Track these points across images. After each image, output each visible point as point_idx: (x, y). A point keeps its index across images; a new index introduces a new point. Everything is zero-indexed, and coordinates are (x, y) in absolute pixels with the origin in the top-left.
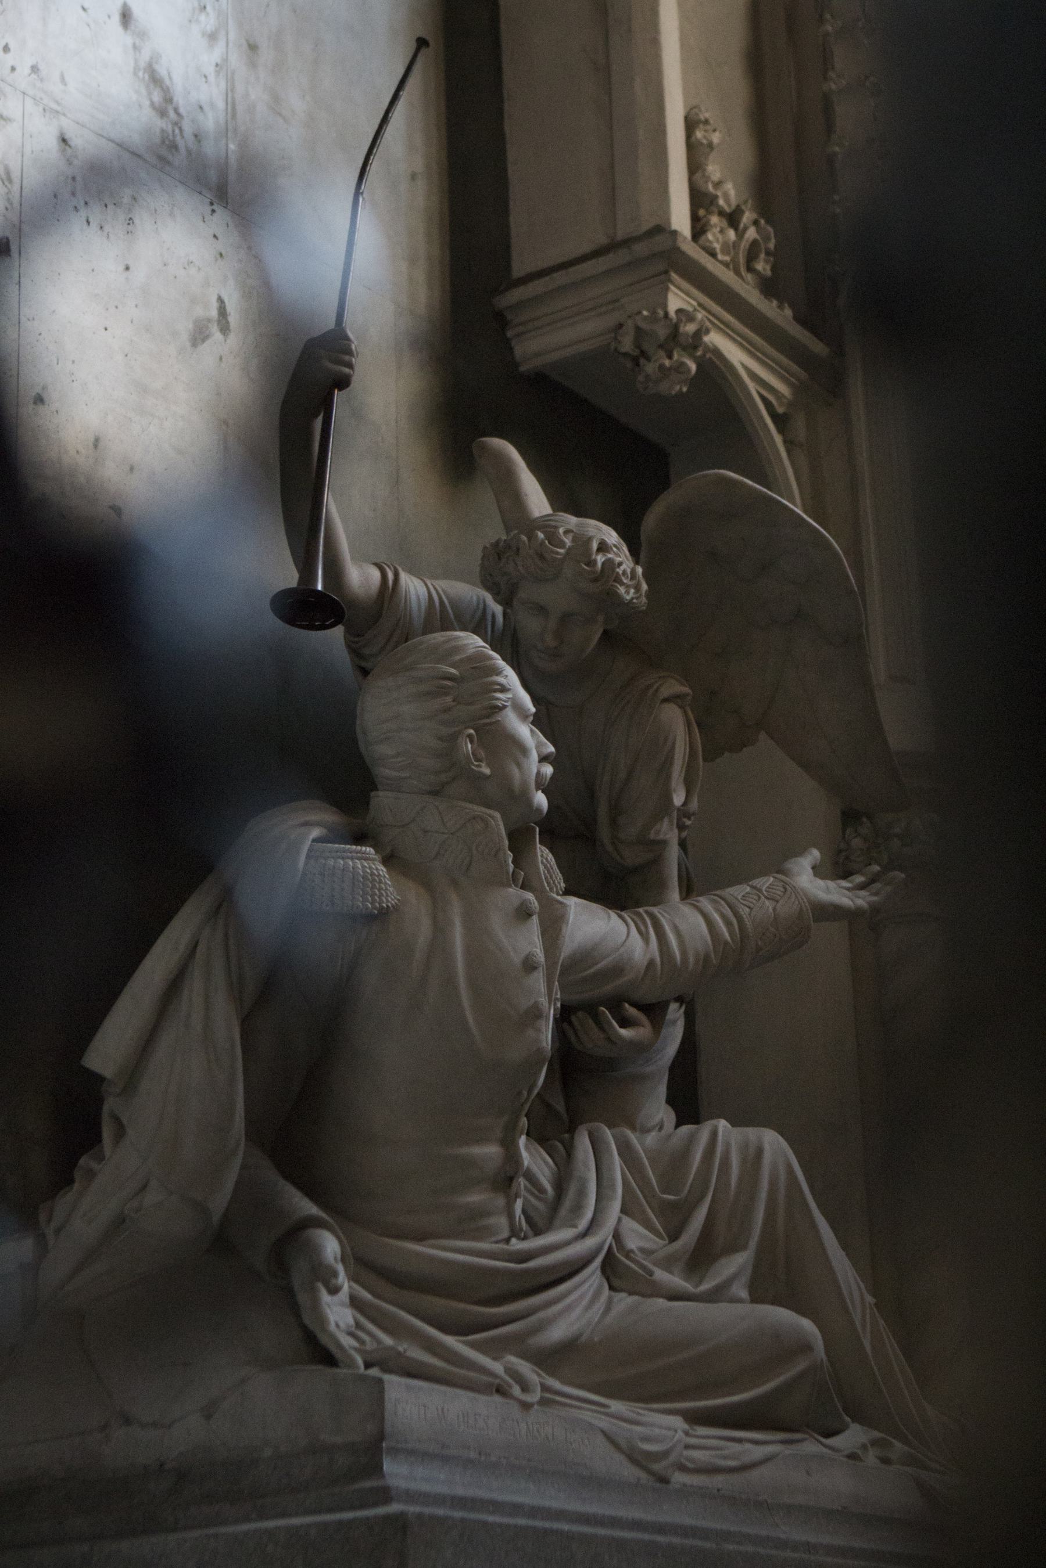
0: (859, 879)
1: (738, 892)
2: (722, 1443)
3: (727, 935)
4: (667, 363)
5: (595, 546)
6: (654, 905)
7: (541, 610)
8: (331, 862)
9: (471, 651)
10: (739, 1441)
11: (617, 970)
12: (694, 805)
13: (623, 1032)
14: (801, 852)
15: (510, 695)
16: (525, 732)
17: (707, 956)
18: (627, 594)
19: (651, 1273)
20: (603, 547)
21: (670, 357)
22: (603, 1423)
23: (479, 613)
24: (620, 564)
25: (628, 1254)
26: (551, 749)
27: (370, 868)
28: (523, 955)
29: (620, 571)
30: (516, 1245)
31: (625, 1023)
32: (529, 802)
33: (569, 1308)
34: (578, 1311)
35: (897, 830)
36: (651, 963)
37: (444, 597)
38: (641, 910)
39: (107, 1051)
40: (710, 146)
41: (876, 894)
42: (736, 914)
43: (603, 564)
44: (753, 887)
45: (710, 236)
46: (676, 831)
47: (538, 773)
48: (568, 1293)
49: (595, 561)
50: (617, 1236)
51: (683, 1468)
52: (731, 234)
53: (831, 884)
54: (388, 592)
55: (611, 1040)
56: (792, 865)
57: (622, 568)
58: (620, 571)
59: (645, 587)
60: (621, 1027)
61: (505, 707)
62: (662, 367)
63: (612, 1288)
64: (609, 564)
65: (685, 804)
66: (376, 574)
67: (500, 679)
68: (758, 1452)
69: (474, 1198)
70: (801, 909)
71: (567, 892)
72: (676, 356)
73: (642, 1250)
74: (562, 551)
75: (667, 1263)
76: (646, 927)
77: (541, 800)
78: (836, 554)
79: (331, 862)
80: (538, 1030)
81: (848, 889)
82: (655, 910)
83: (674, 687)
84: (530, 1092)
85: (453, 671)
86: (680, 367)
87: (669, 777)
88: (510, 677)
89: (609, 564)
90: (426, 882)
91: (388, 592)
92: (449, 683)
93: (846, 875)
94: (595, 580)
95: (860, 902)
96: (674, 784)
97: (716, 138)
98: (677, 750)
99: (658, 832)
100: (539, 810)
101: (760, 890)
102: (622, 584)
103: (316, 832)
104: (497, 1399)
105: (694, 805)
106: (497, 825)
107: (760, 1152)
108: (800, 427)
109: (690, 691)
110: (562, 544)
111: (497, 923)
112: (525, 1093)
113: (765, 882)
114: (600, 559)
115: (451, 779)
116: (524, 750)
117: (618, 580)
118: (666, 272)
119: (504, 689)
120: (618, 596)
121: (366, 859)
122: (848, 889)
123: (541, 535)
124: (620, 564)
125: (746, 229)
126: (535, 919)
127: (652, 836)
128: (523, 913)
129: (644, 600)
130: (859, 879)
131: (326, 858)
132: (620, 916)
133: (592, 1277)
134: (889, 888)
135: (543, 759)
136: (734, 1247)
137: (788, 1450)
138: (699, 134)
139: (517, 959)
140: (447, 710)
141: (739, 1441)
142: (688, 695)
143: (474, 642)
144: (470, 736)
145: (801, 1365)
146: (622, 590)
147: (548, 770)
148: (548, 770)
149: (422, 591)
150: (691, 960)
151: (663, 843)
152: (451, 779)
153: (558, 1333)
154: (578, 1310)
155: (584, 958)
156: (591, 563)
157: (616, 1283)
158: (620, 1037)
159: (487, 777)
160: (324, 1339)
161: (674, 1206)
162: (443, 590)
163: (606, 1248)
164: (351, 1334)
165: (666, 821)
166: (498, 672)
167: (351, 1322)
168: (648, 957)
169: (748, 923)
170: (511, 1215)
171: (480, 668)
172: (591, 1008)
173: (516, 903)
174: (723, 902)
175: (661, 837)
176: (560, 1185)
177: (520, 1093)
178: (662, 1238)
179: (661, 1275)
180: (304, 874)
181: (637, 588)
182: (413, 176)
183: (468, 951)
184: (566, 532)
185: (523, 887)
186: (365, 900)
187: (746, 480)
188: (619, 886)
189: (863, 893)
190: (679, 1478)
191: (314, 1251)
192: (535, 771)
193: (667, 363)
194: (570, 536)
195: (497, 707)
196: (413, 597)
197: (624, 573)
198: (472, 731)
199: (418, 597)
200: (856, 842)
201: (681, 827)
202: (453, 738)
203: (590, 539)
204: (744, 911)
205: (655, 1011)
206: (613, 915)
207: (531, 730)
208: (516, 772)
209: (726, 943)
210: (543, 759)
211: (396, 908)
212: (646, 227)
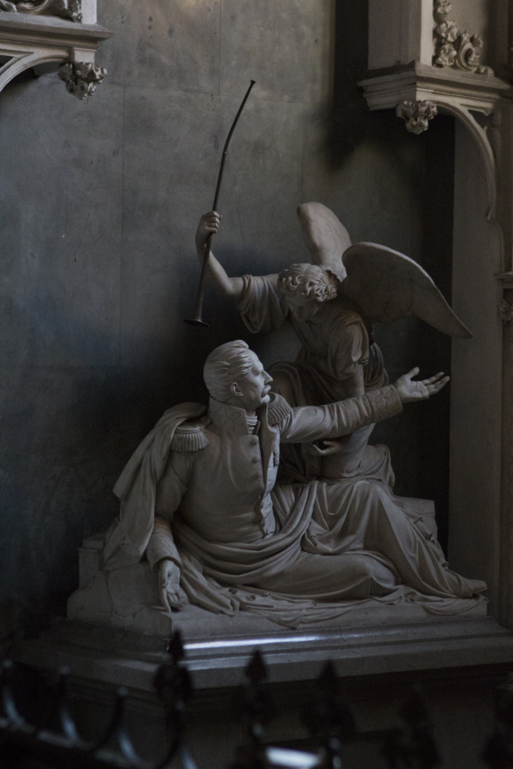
0: (434, 379)
2: (322, 611)
3: (366, 414)
4: (415, 123)
5: (308, 285)
8: (182, 435)
10: (334, 608)
13: (323, 452)
19: (315, 545)
20: (311, 284)
21: (416, 120)
22: (267, 614)
25: (311, 538)
26: (271, 379)
29: (318, 292)
32: (259, 402)
33: (281, 561)
34: (284, 562)
36: (334, 428)
37: (271, 286)
40: (445, 13)
41: (436, 388)
42: (371, 405)
43: (310, 292)
45: (440, 59)
47: (262, 392)
48: (279, 557)
50: (308, 531)
51: (303, 623)
52: (454, 53)
56: (399, 381)
62: (412, 125)
63: (302, 550)
65: (361, 357)
67: (246, 365)
68: (339, 611)
69: (245, 529)
72: (418, 119)
73: (317, 535)
74: (296, 287)
79: (182, 435)
85: (228, 364)
86: (421, 125)
89: (312, 291)
90: (220, 435)
96: (353, 353)
97: (448, 9)
104: (221, 615)
107: (368, 496)
108: (499, 119)
112: (260, 497)
114: (309, 289)
115: (229, 400)
116: (255, 386)
117: (317, 295)
118: (415, 83)
122: (426, 385)
125: (464, 45)
127: (346, 371)
128: (253, 444)
131: (180, 434)
133: (297, 546)
136: (353, 532)
137: (357, 607)
138: (439, 10)
139: (250, 460)
140: (226, 377)
141: (334, 608)
145: (362, 580)
147: (269, 388)
152: (229, 400)
153: (274, 571)
154: (279, 565)
156: (305, 292)
157: (305, 548)
161: (333, 517)
163: (302, 534)
165: (352, 366)
169: (375, 409)
170: (262, 531)
171: (238, 362)
174: (367, 400)
175: (350, 371)
176: (294, 508)
177: (257, 498)
178: (326, 528)
179: (321, 546)
180: (173, 439)
182: (316, 41)
184: (299, 278)
189: (432, 386)
190: (301, 626)
192: (261, 391)
193: (415, 123)
196: (256, 288)
198: (235, 383)
202: (228, 387)
204: (374, 404)
208: (253, 394)
209: (366, 417)
210: (266, 384)
211: (208, 446)
212: (410, 60)
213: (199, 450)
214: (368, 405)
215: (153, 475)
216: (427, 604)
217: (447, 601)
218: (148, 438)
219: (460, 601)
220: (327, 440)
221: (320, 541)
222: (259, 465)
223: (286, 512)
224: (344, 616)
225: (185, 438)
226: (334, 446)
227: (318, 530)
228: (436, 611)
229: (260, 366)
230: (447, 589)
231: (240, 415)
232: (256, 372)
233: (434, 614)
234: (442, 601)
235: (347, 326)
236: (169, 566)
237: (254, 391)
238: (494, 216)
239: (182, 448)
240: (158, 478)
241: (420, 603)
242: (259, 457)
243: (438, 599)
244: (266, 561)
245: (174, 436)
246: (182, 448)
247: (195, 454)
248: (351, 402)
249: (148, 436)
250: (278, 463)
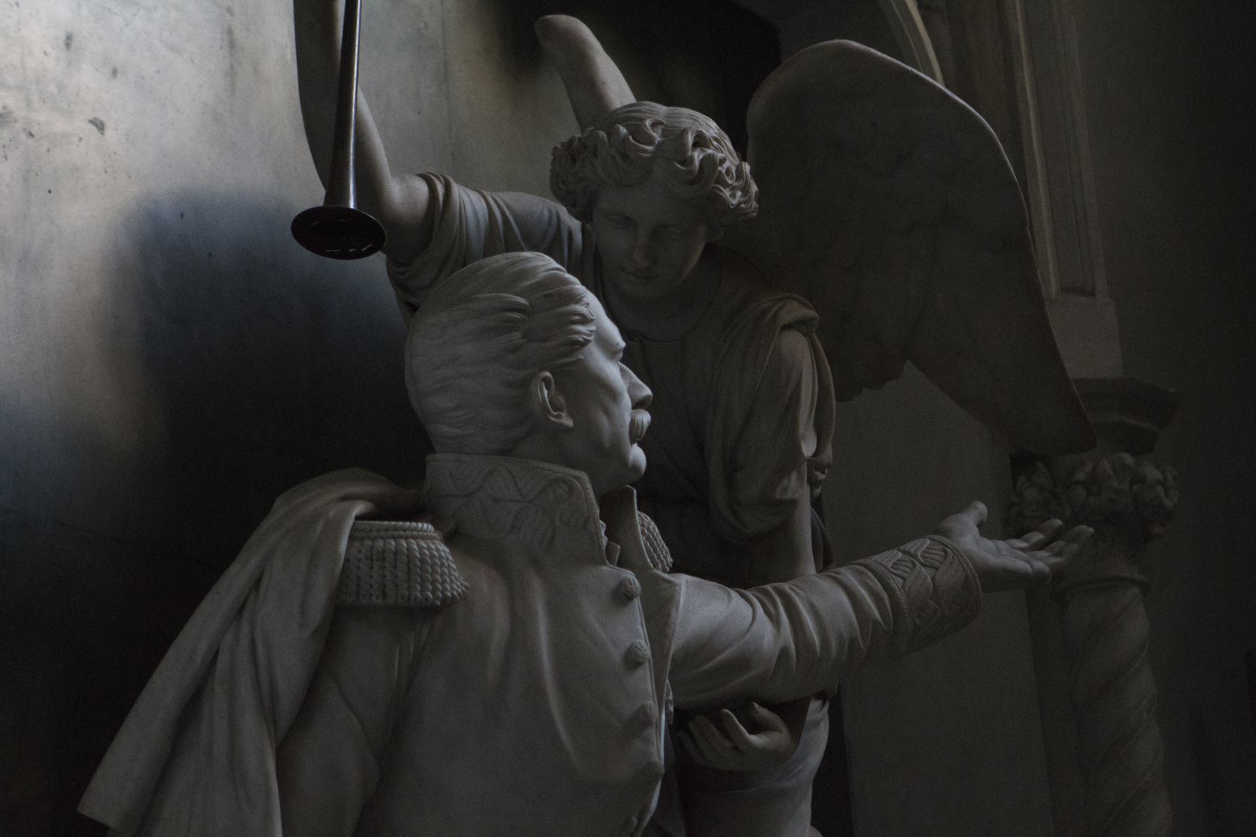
0: (1037, 537)
1: (887, 559)
5: (690, 139)
6: (785, 580)
7: (627, 222)
9: (542, 275)
11: (742, 662)
12: (828, 454)
13: (753, 738)
14: (962, 508)
16: (613, 371)
17: (853, 641)
18: (733, 198)
20: (701, 141)
23: (552, 231)
24: (722, 161)
26: (647, 391)
27: (429, 549)
29: (723, 169)
31: (755, 728)
35: (1081, 476)
36: (784, 652)
38: (769, 587)
39: (110, 792)
41: (1059, 554)
43: (702, 161)
44: (904, 552)
46: (807, 488)
47: (633, 422)
49: (692, 158)
53: (1002, 545)
54: (439, 210)
55: (741, 749)
56: (951, 523)
57: (726, 165)
58: (723, 169)
59: (754, 188)
60: (750, 733)
61: (587, 342)
64: (709, 162)
65: (815, 455)
66: (423, 188)
67: (580, 308)
70: (967, 578)
71: (675, 569)
74: (650, 148)
76: (776, 607)
77: (637, 454)
78: (990, 138)
79: (380, 543)
80: (647, 741)
81: (1023, 550)
82: (786, 586)
83: (794, 310)
84: (640, 820)
85: (522, 300)
87: (795, 421)
88: (592, 304)
89: (709, 162)
90: (499, 563)
91: (439, 210)
92: (517, 316)
93: (1019, 535)
94: (692, 182)
95: (1039, 565)
96: (801, 430)
99: (786, 489)
100: (635, 468)
101: (915, 556)
102: (726, 185)
103: (359, 508)
105: (828, 454)
106: (585, 488)
109: (814, 314)
110: (650, 141)
111: (591, 611)
112: (635, 820)
113: (921, 546)
114: (697, 156)
115: (524, 435)
116: (614, 395)
117: (720, 180)
119: (585, 320)
120: (723, 201)
121: (423, 538)
122: (1023, 550)
123: (623, 130)
124: (722, 161)
126: (637, 602)
127: (778, 496)
128: (622, 596)
129: (755, 204)
130: (1037, 537)
132: (743, 596)
134: (1075, 546)
135: (638, 405)
139: (617, 654)
140: (515, 349)
142: (813, 319)
143: (546, 264)
144: (546, 380)
146: (727, 193)
148: (645, 418)
149: (481, 206)
150: (834, 645)
151: (793, 503)
152: (524, 435)
155: (701, 648)
156: (687, 161)
158: (750, 745)
159: (568, 430)
162: (508, 207)
165: (794, 476)
166: (578, 299)
168: (781, 643)
169: (901, 595)
172: (712, 712)
173: (613, 583)
174: (870, 574)
175: (789, 495)
177: (628, 821)
180: (347, 560)
181: (745, 189)
183: (555, 646)
185: (621, 564)
186: (422, 592)
187: (873, 50)
188: (742, 559)
189: (1043, 554)
192: (628, 419)
194: (660, 129)
195: (577, 342)
196: (470, 214)
197: (728, 171)
198: (548, 374)
199: (476, 213)
200: (1031, 494)
201: (813, 483)
202: (524, 385)
203: (684, 132)
204: (896, 583)
205: (792, 712)
206: (733, 593)
207: (622, 370)
208: (604, 421)
209: (876, 622)
210: (638, 405)
211: (464, 597)
213: (445, 600)
214: (878, 586)
215: (268, 709)
218: (236, 577)
225: (396, 553)
226: (776, 729)
231: (571, 488)
239: (384, 595)
242: (646, 649)
245: (348, 548)
246: (384, 595)
247: (426, 615)
249: (234, 569)
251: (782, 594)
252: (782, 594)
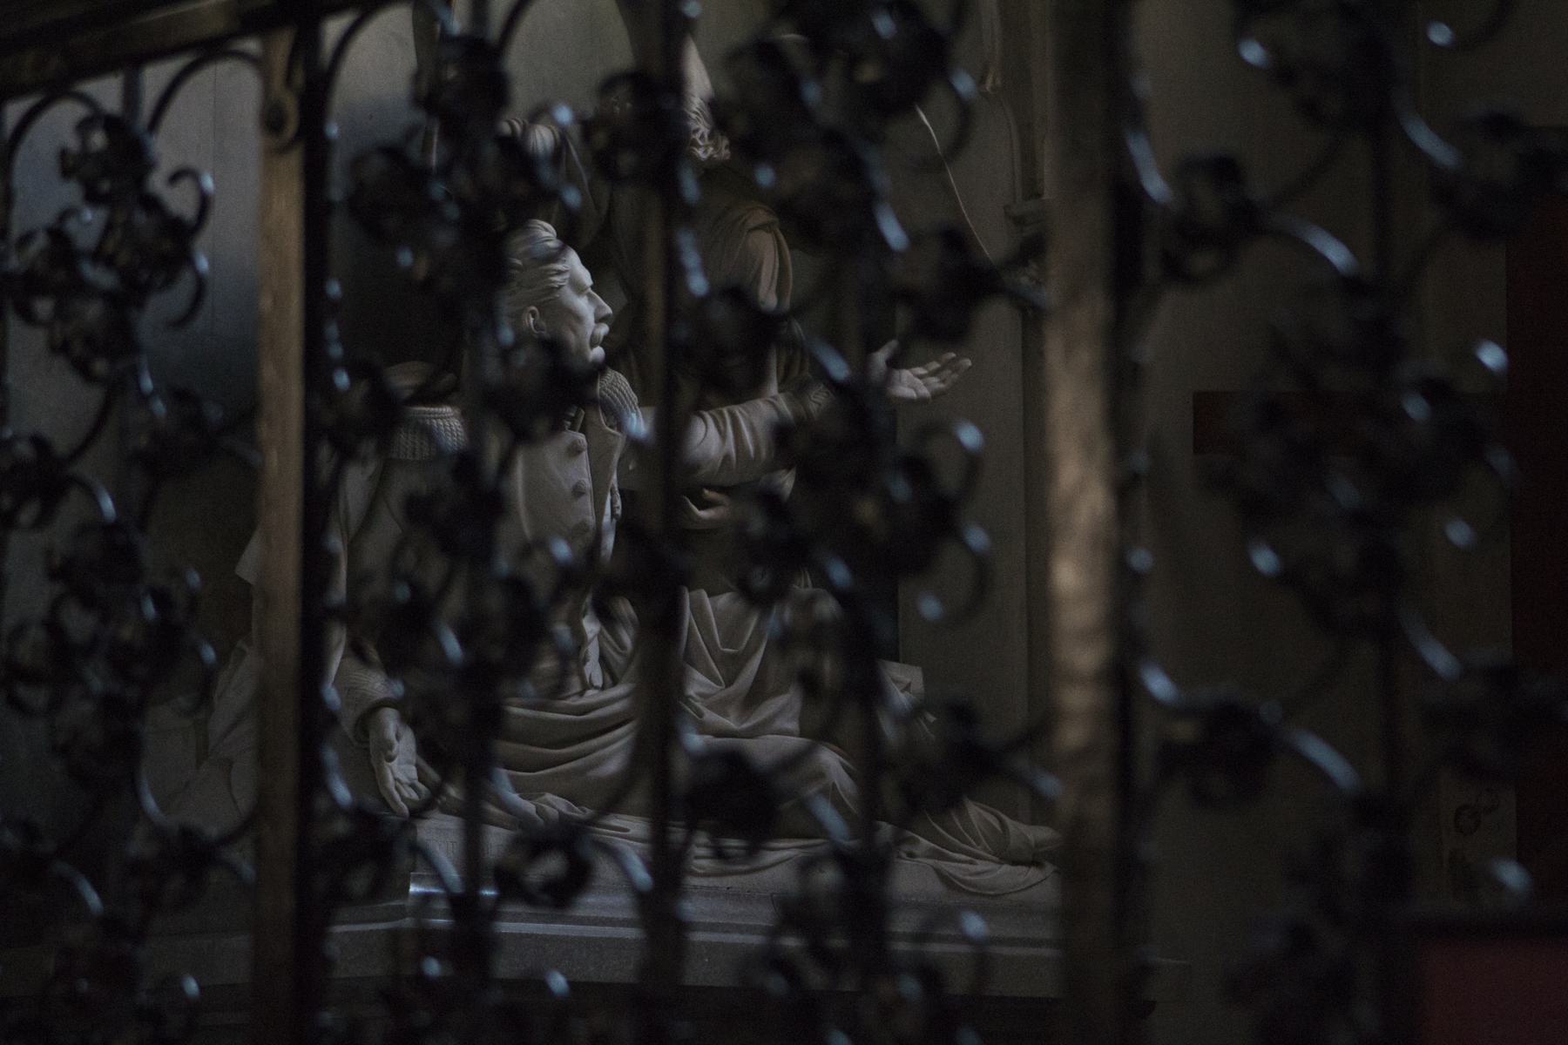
0: (935, 365)
6: (737, 402)
13: (704, 514)
15: (567, 276)
19: (701, 715)
26: (609, 310)
28: (572, 484)
29: (697, 136)
30: (591, 696)
31: (705, 505)
36: (727, 457)
41: (943, 381)
58: (697, 136)
73: (701, 695)
75: (720, 706)
81: (921, 377)
82: (737, 409)
93: (922, 364)
95: (925, 392)
98: (764, 269)
116: (579, 319)
117: (695, 144)
119: (560, 273)
122: (921, 377)
126: (585, 453)
128: (574, 451)
130: (935, 365)
134: (955, 376)
135: (600, 320)
139: (567, 487)
147: (604, 329)
160: (385, 795)
161: (733, 657)
164: (413, 786)
167: (414, 774)
179: (710, 716)
189: (934, 380)
191: (381, 728)
192: (589, 333)
210: (600, 320)
216: (945, 866)
217: (981, 866)
219: (1006, 868)
220: (710, 487)
221: (710, 707)
222: (587, 503)
223: (623, 647)
224: (774, 870)
227: (701, 684)
228: (964, 882)
229: (586, 277)
230: (977, 839)
232: (578, 288)
233: (960, 890)
234: (971, 863)
235: (751, 230)
236: (391, 721)
237: (574, 331)
238: (999, 82)
240: (353, 530)
241: (931, 861)
242: (587, 483)
243: (963, 857)
244: (594, 742)
248: (760, 403)
250: (619, 512)
251: (733, 416)
252: (733, 416)
